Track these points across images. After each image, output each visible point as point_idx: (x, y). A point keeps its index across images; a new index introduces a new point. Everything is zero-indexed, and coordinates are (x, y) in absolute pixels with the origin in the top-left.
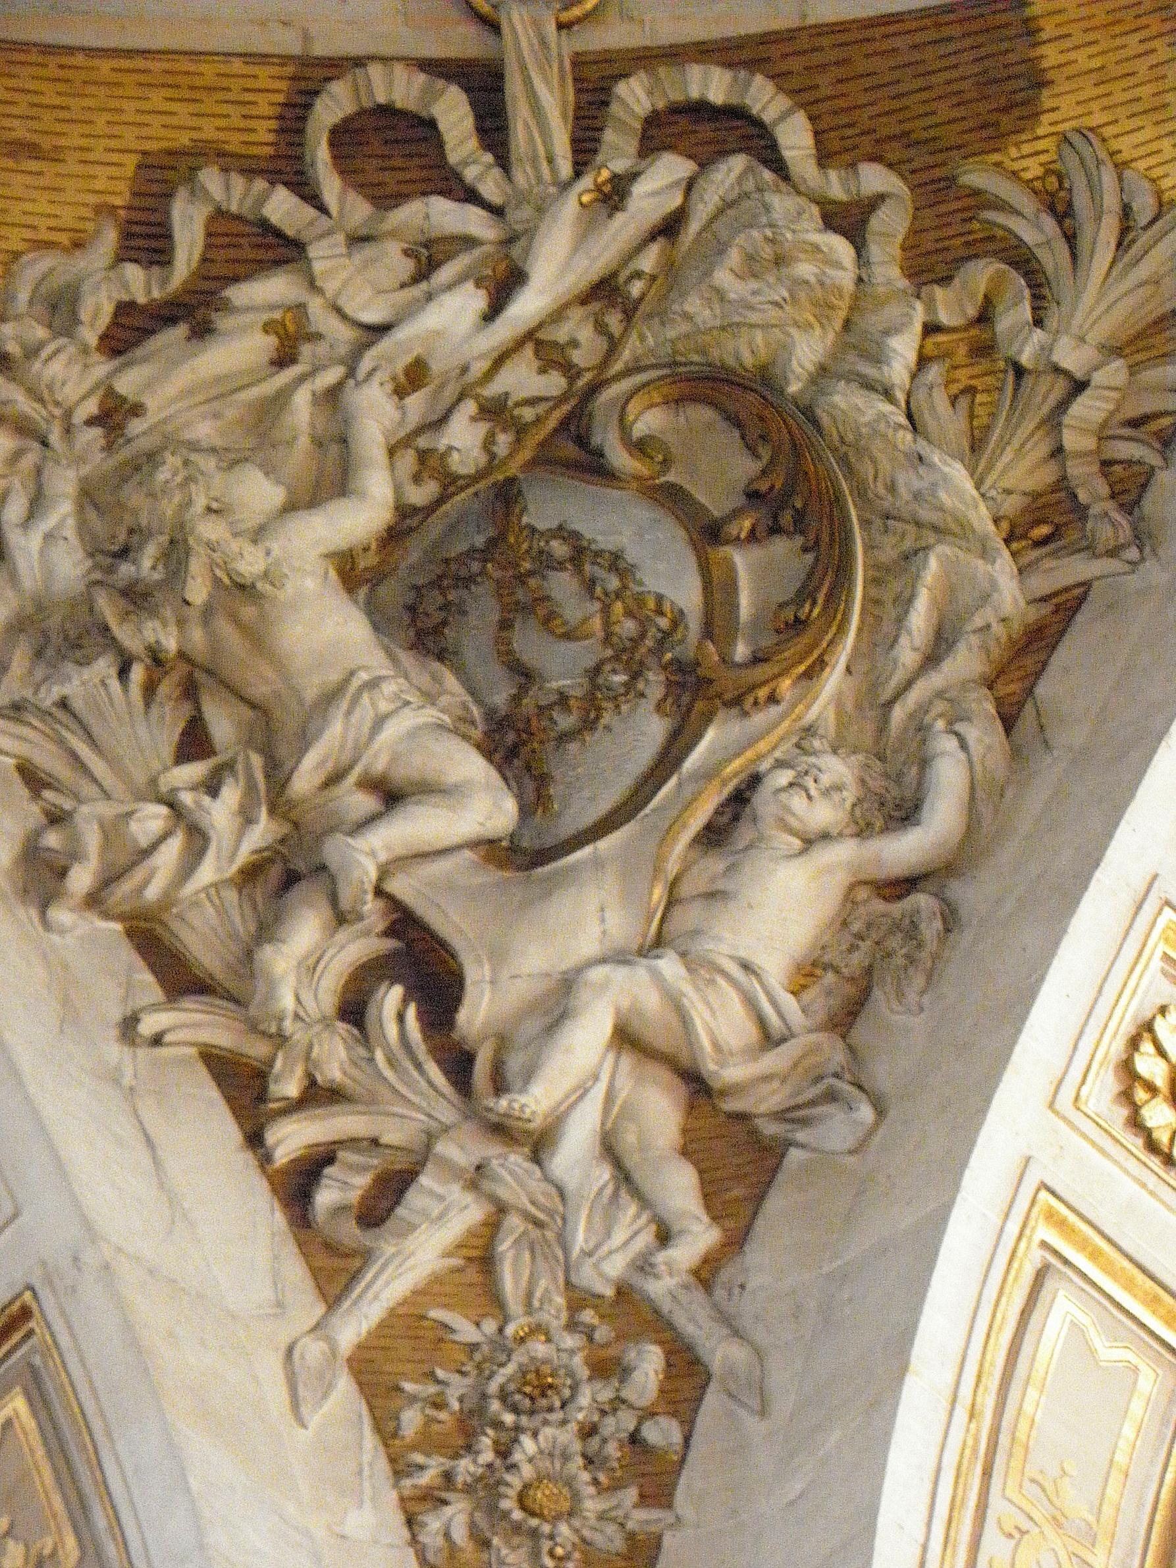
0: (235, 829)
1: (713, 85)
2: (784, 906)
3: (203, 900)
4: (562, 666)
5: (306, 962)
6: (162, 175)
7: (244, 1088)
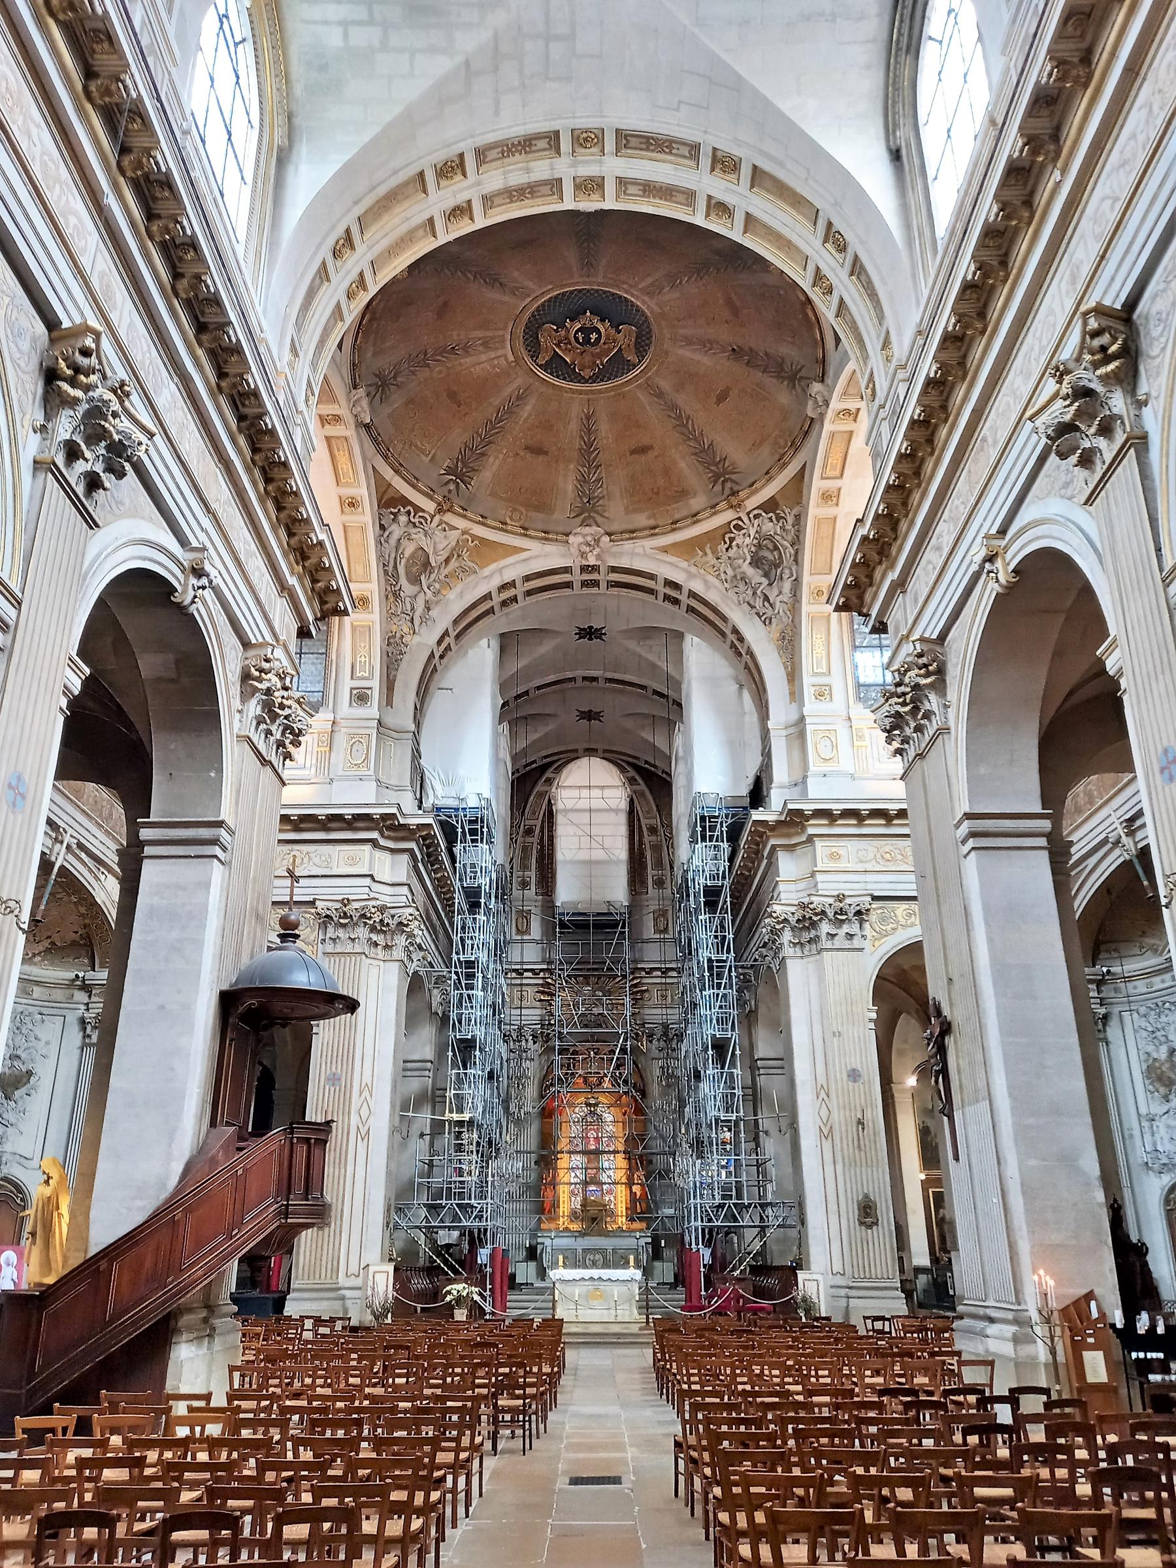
0: (750, 592)
1: (756, 512)
2: (787, 586)
3: (749, 598)
4: (766, 568)
5: (758, 603)
7: (758, 614)
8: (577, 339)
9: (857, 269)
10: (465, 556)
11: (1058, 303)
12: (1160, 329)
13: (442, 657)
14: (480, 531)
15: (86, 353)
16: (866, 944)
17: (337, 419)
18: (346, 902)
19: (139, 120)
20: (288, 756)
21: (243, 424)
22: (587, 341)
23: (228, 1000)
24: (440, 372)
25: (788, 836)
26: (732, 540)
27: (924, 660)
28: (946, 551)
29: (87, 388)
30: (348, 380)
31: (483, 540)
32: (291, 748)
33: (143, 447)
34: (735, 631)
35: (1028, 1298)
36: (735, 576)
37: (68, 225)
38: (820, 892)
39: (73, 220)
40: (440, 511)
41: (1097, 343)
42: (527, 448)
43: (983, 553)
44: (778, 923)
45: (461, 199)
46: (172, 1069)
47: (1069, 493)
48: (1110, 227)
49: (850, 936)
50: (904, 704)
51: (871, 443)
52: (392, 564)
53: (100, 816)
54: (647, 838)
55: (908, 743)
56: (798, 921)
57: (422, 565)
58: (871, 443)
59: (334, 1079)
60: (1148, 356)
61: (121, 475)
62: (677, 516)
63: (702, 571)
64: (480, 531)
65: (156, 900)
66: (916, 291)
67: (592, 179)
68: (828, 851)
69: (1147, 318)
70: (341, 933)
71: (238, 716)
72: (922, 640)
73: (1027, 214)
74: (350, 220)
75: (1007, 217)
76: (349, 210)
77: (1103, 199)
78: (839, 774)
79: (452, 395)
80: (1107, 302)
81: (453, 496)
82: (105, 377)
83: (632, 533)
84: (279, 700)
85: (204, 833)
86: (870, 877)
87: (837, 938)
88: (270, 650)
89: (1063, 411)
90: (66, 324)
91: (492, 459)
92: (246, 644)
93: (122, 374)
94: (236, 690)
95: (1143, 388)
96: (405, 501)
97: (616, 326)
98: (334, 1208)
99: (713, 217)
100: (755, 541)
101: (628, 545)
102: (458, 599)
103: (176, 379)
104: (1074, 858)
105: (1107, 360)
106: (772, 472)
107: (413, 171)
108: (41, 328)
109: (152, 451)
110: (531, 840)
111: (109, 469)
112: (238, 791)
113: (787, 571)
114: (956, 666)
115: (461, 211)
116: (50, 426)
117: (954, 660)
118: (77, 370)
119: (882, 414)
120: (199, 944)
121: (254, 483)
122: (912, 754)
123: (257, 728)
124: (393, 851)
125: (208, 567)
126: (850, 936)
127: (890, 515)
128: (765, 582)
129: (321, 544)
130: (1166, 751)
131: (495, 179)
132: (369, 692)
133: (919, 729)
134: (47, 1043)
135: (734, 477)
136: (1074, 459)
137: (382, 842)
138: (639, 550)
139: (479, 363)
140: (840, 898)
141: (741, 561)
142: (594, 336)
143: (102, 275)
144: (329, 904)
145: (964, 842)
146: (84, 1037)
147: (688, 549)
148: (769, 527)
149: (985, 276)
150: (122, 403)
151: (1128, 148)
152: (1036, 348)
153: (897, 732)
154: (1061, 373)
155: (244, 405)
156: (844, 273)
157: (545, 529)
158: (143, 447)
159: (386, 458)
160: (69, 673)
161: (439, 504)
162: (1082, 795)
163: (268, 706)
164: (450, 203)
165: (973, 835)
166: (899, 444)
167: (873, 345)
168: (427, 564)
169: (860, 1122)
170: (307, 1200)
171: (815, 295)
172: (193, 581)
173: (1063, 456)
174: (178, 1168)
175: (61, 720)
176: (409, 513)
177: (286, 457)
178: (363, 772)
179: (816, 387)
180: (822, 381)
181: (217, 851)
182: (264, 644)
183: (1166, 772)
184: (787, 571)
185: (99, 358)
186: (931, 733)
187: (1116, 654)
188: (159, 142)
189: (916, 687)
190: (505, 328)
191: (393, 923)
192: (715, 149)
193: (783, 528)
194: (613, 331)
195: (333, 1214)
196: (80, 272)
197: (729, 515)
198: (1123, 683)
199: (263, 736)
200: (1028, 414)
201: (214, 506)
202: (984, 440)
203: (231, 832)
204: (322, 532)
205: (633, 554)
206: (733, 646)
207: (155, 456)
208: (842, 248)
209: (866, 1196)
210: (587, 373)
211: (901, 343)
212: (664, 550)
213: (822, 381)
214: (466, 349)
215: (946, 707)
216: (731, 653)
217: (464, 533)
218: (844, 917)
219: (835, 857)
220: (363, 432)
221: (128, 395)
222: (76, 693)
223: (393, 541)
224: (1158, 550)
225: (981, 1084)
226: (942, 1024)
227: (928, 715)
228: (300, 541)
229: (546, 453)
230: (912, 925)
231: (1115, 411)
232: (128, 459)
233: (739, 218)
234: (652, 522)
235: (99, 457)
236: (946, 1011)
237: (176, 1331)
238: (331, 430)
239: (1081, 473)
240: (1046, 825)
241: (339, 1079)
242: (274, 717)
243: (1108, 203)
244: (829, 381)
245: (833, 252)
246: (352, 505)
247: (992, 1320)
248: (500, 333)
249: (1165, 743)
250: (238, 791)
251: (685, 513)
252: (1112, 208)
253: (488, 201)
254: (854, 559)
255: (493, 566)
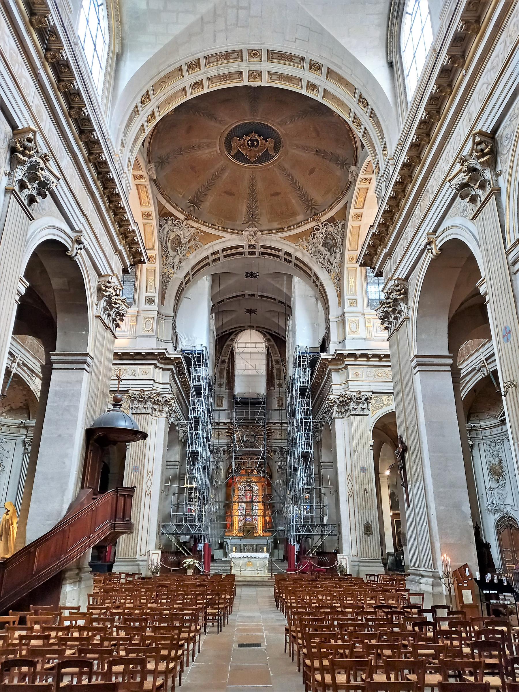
0: (322, 258)
1: (325, 223)
2: (338, 255)
5: (326, 263)
6: (311, 233)
7: (325, 268)
8: (248, 144)
9: (372, 115)
10: (197, 239)
11: (462, 130)
12: (507, 142)
13: (186, 284)
14: (204, 228)
15: (29, 140)
16: (370, 413)
17: (141, 177)
18: (142, 391)
19: (55, 36)
20: (118, 325)
21: (100, 176)
22: (253, 145)
23: (89, 433)
24: (187, 157)
25: (337, 365)
26: (315, 235)
27: (399, 288)
28: (409, 240)
29: (30, 157)
30: (147, 160)
31: (205, 233)
32: (119, 322)
33: (55, 184)
34: (315, 275)
35: (439, 568)
36: (316, 251)
37: (21, 82)
38: (350, 390)
39: (24, 81)
40: (186, 219)
41: (479, 147)
42: (225, 192)
43: (426, 240)
44: (332, 403)
45: (198, 79)
46: (64, 463)
47: (465, 214)
48: (486, 96)
49: (363, 409)
50: (389, 307)
51: (377, 192)
52: (164, 242)
53: (33, 351)
54: (275, 366)
55: (391, 324)
56: (340, 402)
57: (178, 243)
58: (377, 192)
59: (136, 469)
60: (502, 154)
61: (44, 196)
62: (291, 224)
63: (301, 248)
64: (204, 228)
65: (58, 388)
66: (398, 126)
67: (256, 72)
68: (353, 372)
69: (501, 137)
70: (140, 405)
71: (95, 307)
72: (398, 279)
73: (449, 90)
74: (148, 87)
75: (441, 91)
76: (148, 82)
77: (483, 84)
78: (360, 338)
79: (193, 168)
80: (484, 130)
81: (192, 213)
82: (38, 152)
83: (271, 231)
84: (114, 300)
85: (80, 358)
86: (372, 384)
87: (357, 410)
88: (110, 278)
89: (463, 178)
90: (20, 127)
91: (209, 197)
92: (100, 275)
93: (44, 150)
94: (95, 295)
95: (499, 168)
96: (171, 215)
97: (265, 139)
98: (135, 525)
99: (309, 90)
100: (325, 236)
101: (269, 236)
102: (194, 258)
103: (70, 155)
104: (462, 375)
105: (484, 155)
106: (333, 205)
107: (177, 65)
108: (9, 129)
109: (58, 186)
110: (224, 365)
111: (39, 194)
112: (95, 341)
113: (338, 249)
114: (413, 291)
115: (198, 85)
116: (12, 173)
117: (412, 288)
118: (25, 148)
119: (382, 179)
120: (77, 408)
121: (104, 203)
122: (392, 329)
123: (104, 313)
124: (163, 369)
125: (83, 240)
126: (363, 409)
127: (385, 224)
128: (329, 253)
129: (133, 231)
130: (505, 328)
131: (213, 71)
132: (154, 299)
133: (396, 318)
134: (8, 452)
135: (315, 207)
136: (468, 199)
137: (159, 365)
138: (274, 239)
139: (204, 154)
140: (359, 392)
141: (318, 244)
142: (256, 143)
143: (37, 106)
144: (135, 392)
145: (414, 368)
146: (25, 449)
147: (295, 238)
148: (330, 229)
149: (430, 118)
150: (45, 164)
151: (495, 61)
152: (452, 150)
153: (386, 320)
154: (463, 161)
155: (100, 167)
156: (366, 117)
157: (233, 228)
158: (55, 184)
159: (163, 195)
160: (20, 284)
161: (186, 216)
162: (464, 349)
163: (109, 303)
164: (193, 81)
165: (419, 365)
166: (390, 192)
167: (379, 149)
168: (180, 242)
169: (366, 490)
170: (124, 521)
171: (353, 127)
172: (76, 246)
173: (463, 198)
174: (66, 507)
175: (16, 306)
176: (172, 219)
177: (119, 191)
178: (150, 334)
179: (353, 168)
180: (356, 165)
181: (86, 367)
182: (108, 275)
183: (506, 337)
184: (338, 249)
185: (35, 143)
186: (401, 320)
187: (485, 285)
188: (63, 46)
189: (395, 300)
190: (217, 139)
191: (163, 401)
192: (311, 60)
193: (337, 230)
194: (264, 141)
195: (134, 528)
196: (27, 104)
197: (313, 224)
198: (487, 298)
199: (107, 316)
200: (448, 179)
201: (86, 212)
202: (428, 191)
203: (92, 359)
204: (134, 226)
205: (271, 240)
206: (314, 281)
207: (60, 189)
208: (366, 105)
209: (368, 522)
210: (252, 160)
211: (391, 148)
212: (285, 238)
213: (356, 165)
214: (199, 147)
215: (408, 309)
216: (313, 285)
217: (197, 229)
218: (360, 401)
219: (356, 374)
220: (153, 183)
221: (48, 161)
222: (23, 294)
223: (165, 232)
224: (504, 240)
225: (420, 473)
226: (403, 447)
227: (400, 312)
228: (124, 230)
229: (234, 195)
230: (390, 405)
231: (486, 178)
232: (48, 190)
233: (321, 91)
234: (280, 226)
235: (33, 188)
236: (405, 441)
237: (64, 579)
238: (138, 182)
239: (470, 206)
240: (450, 361)
241: (138, 469)
242: (112, 308)
243: (486, 85)
244: (359, 165)
245: (362, 107)
246: (147, 215)
247: (423, 576)
248: (215, 140)
249: (505, 324)
250: (95, 341)
251: (294, 222)
252: (487, 88)
253: (210, 80)
254: (369, 243)
255: (210, 244)
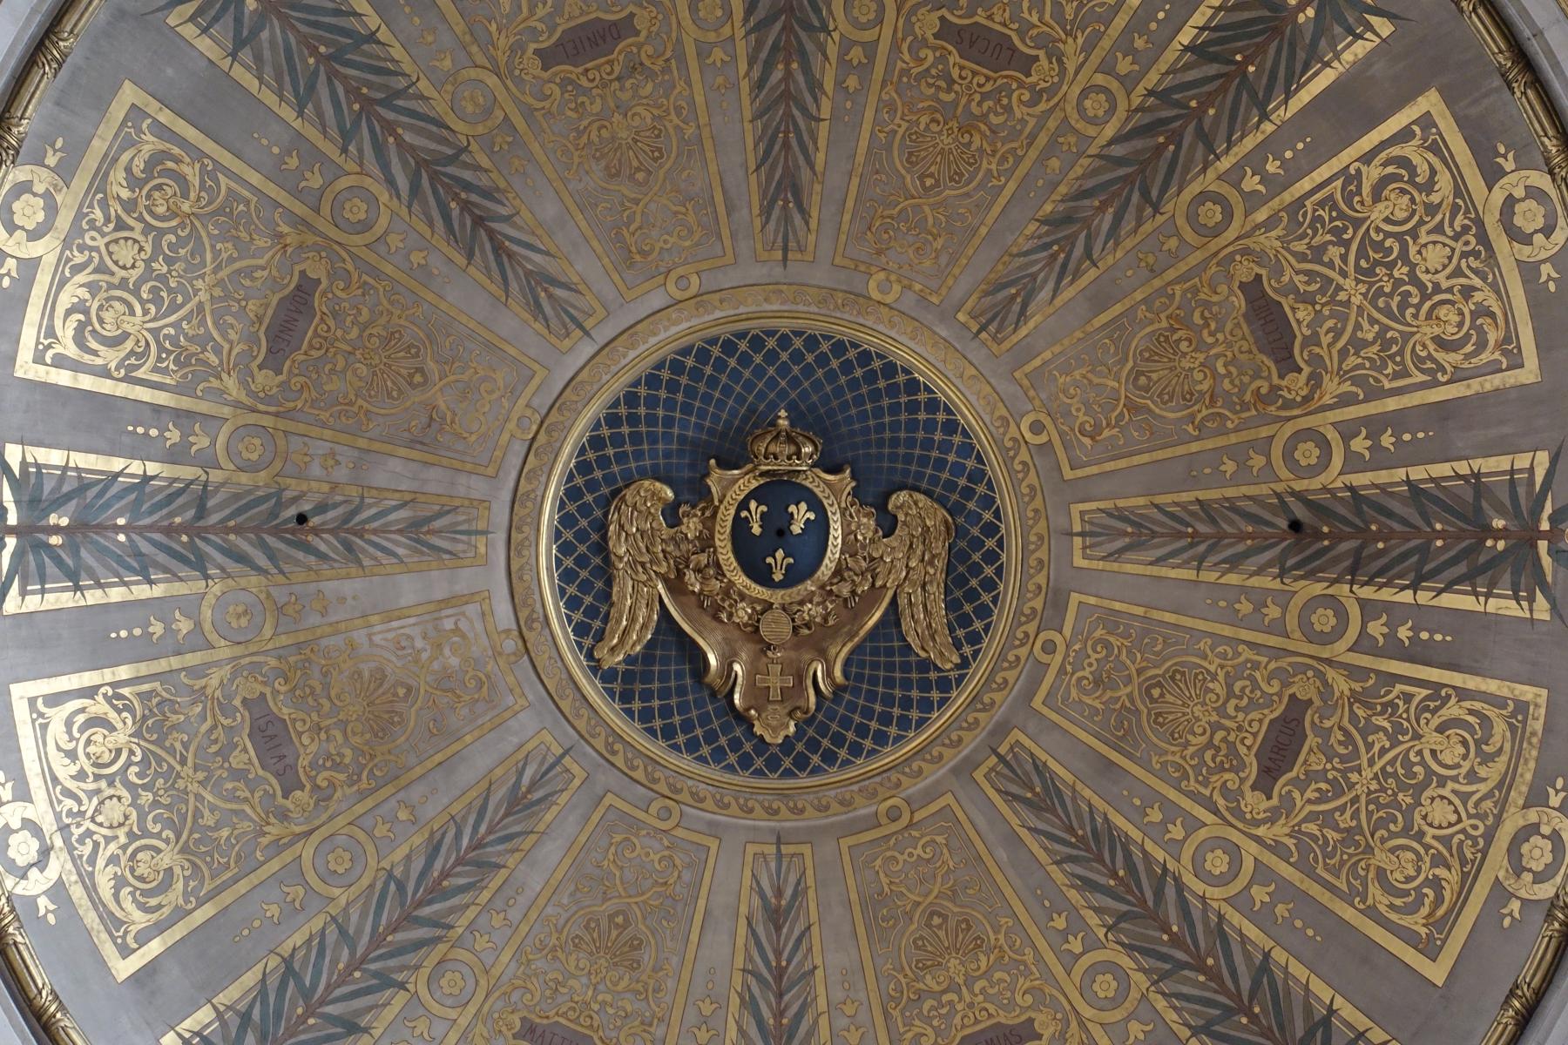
194: (867, 525)
248: (477, 487)
